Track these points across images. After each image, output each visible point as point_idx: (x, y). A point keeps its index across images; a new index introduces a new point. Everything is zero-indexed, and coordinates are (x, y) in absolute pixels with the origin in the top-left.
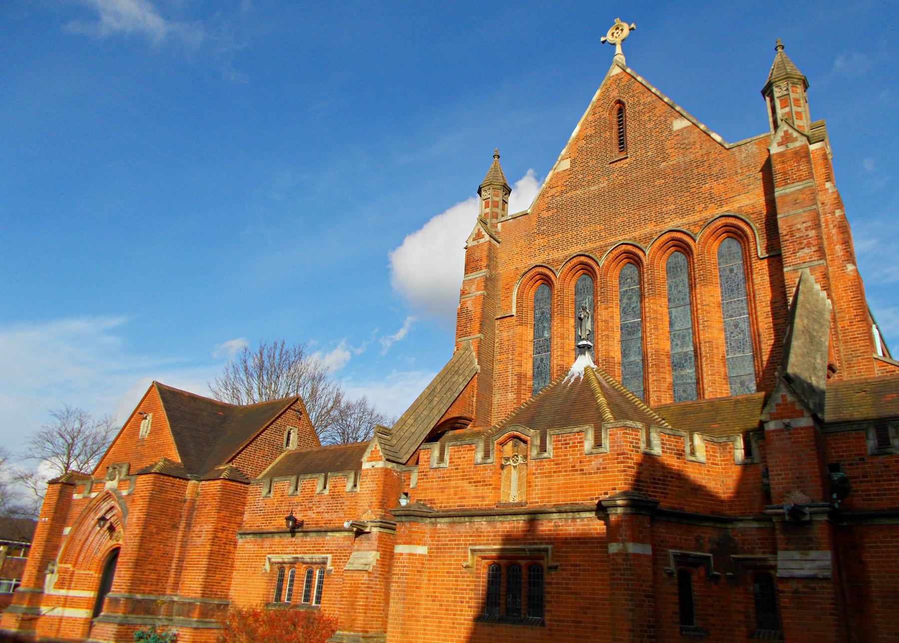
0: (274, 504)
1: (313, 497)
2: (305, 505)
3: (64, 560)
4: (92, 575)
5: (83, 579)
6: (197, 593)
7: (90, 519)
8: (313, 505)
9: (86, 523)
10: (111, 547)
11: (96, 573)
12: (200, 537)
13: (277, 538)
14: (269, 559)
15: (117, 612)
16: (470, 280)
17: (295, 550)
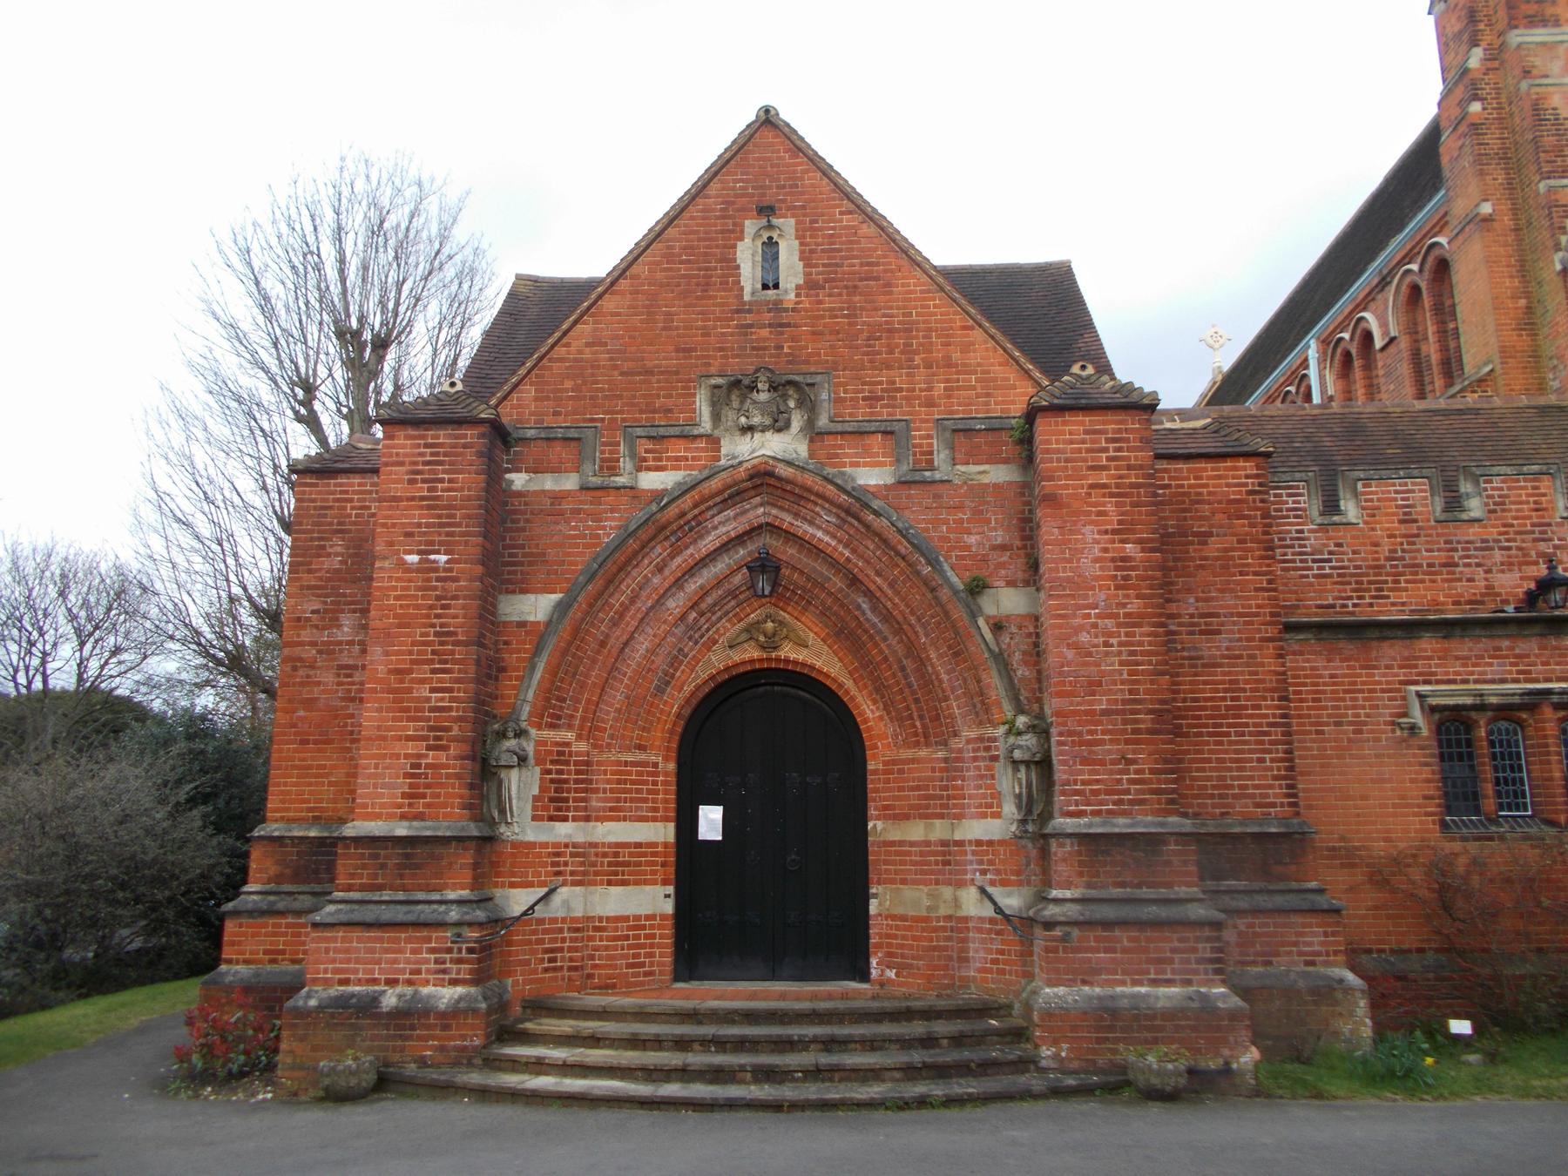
0: (1376, 544)
1: (1549, 525)
2: (1519, 548)
3: (551, 712)
4: (655, 765)
5: (633, 782)
6: (1273, 805)
7: (646, 567)
8: (1556, 547)
9: (628, 586)
10: (727, 669)
11: (666, 759)
12: (1219, 632)
13: (1427, 644)
14: (1419, 695)
15: (1169, 885)
16: (1544, 44)
17: (1519, 672)
